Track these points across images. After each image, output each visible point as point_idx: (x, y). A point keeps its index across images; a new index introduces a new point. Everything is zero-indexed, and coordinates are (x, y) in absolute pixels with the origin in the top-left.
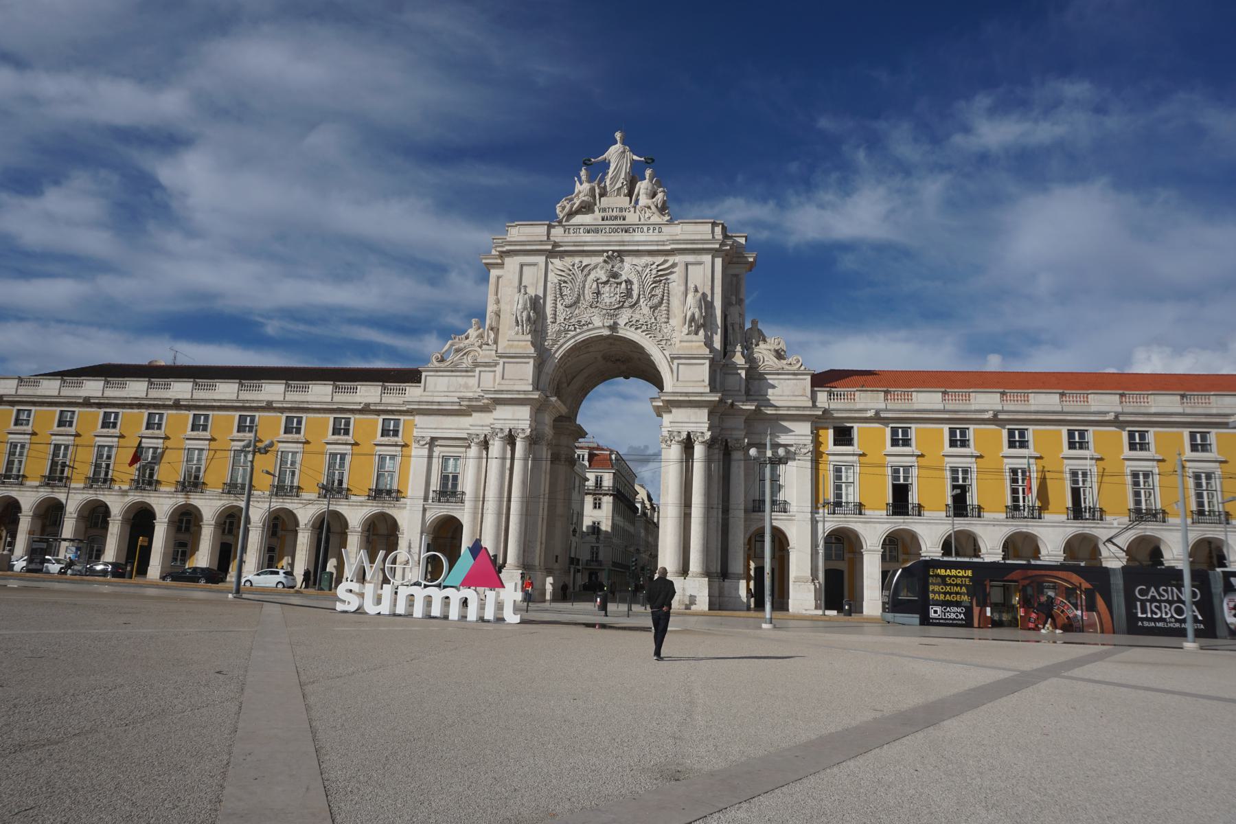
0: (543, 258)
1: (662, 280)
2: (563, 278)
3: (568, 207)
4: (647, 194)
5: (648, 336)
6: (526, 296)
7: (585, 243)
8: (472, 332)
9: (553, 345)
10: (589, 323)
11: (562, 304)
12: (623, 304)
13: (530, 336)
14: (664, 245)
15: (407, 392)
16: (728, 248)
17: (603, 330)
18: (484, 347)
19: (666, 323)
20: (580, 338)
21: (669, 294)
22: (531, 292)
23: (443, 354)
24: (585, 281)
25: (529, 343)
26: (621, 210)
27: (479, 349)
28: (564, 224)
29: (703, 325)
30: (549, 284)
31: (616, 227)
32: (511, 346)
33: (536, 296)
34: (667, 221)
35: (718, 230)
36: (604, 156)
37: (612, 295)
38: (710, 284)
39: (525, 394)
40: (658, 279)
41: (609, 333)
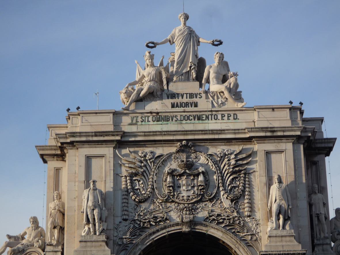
0: (112, 149)
1: (241, 171)
2: (134, 171)
10: (166, 219)
12: (201, 199)
19: (249, 216)
26: (191, 96)
37: (190, 188)
40: (237, 169)
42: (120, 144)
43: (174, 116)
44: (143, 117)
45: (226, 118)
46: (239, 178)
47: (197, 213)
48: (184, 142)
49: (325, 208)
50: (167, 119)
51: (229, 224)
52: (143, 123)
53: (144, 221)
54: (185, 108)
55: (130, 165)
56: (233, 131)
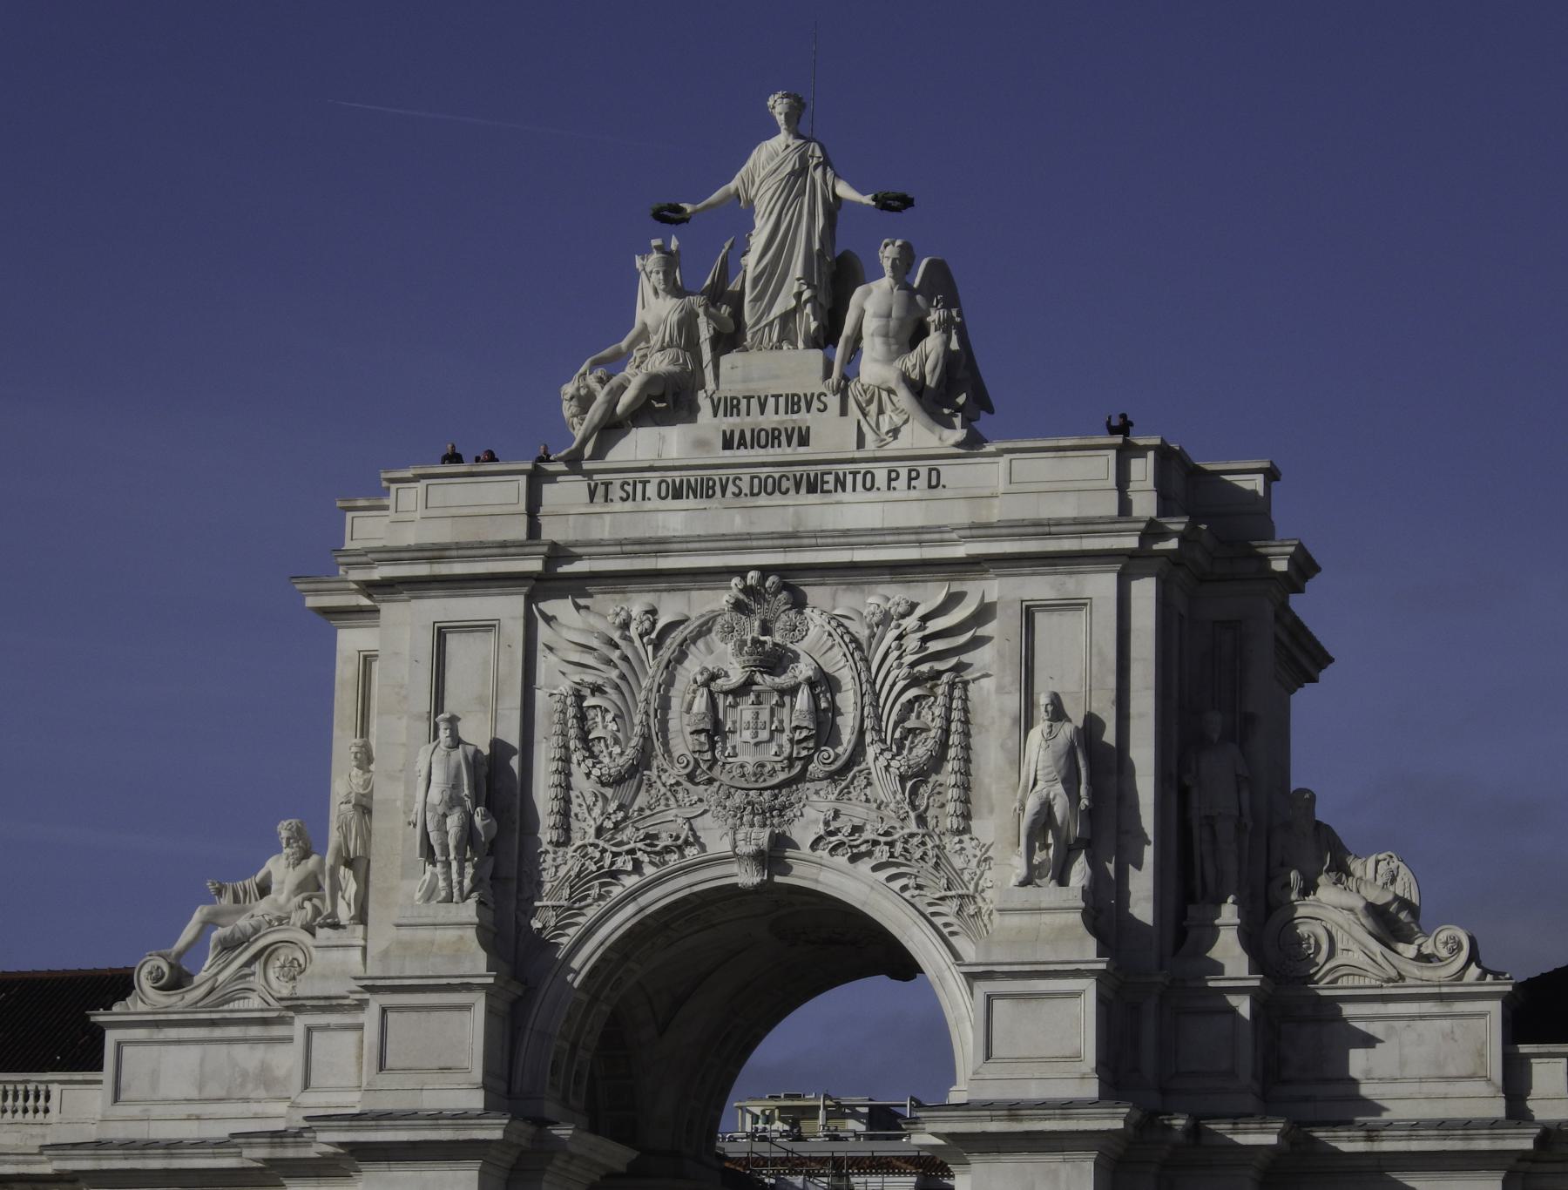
1: (939, 674)
2: (589, 678)
3: (601, 395)
4: (886, 335)
5: (897, 885)
6: (458, 754)
7: (660, 546)
8: (282, 870)
9: (561, 928)
10: (687, 843)
11: (588, 775)
13: (472, 903)
14: (942, 542)
15: (54, 1103)
16: (1173, 544)
17: (734, 868)
18: (323, 933)
19: (959, 832)
20: (657, 898)
21: (966, 722)
22: (477, 735)
23: (180, 955)
24: (670, 682)
25: (471, 933)
26: (793, 403)
27: (305, 937)
28: (587, 465)
29: (1088, 844)
30: (540, 696)
31: (776, 472)
32: (405, 946)
33: (496, 744)
34: (958, 445)
35: (1143, 470)
36: (732, 185)
37: (764, 735)
38: (1112, 681)
39: (456, 1128)
40: (925, 668)
41: (756, 880)
42: (541, 587)
43: (731, 478)
44: (629, 485)
45: (901, 483)
46: (932, 699)
47: (790, 821)
48: (751, 574)
49: (1245, 795)
50: (704, 490)
51: (890, 860)
52: (629, 505)
53: (615, 849)
54: (770, 450)
55: (576, 657)
56: (913, 537)
